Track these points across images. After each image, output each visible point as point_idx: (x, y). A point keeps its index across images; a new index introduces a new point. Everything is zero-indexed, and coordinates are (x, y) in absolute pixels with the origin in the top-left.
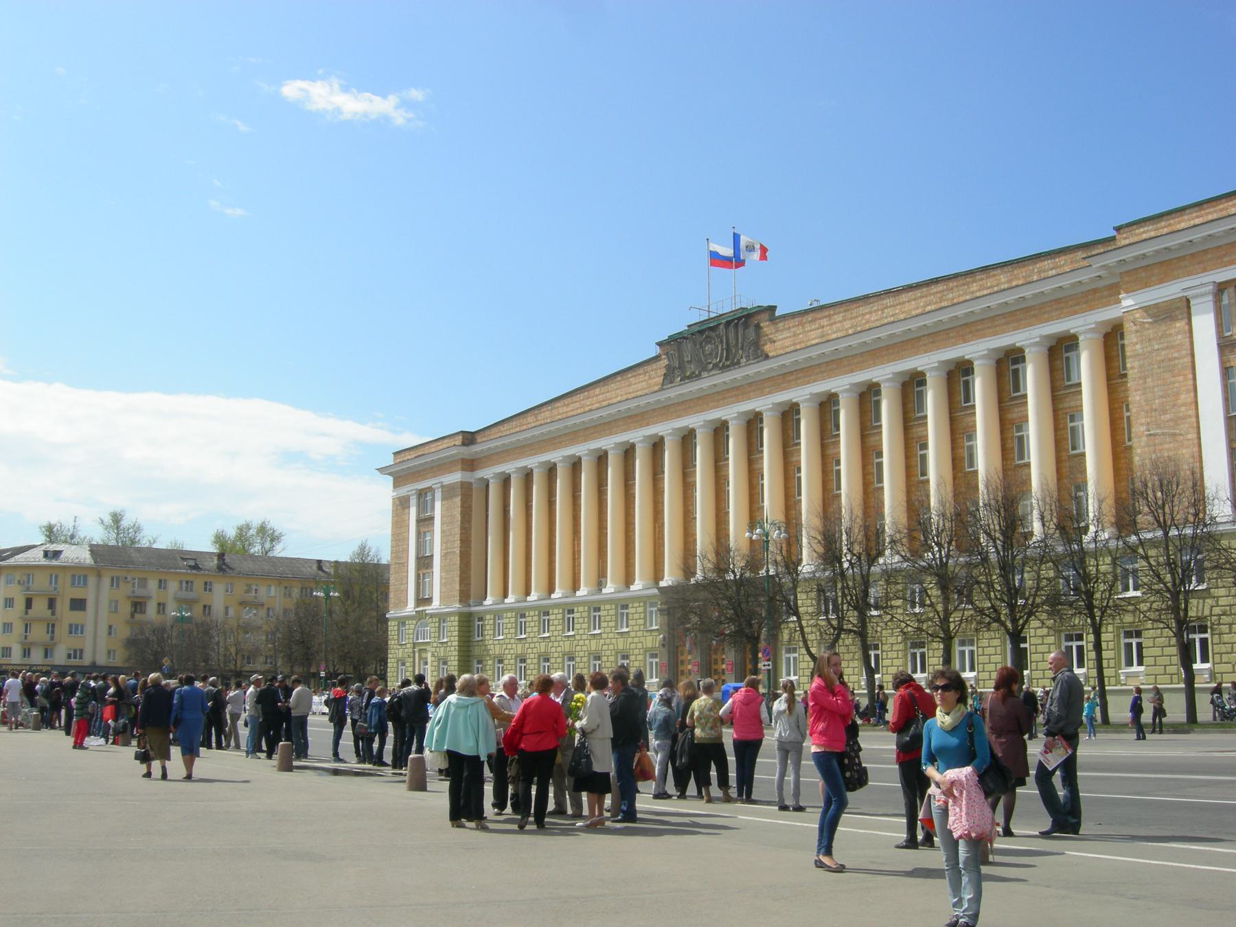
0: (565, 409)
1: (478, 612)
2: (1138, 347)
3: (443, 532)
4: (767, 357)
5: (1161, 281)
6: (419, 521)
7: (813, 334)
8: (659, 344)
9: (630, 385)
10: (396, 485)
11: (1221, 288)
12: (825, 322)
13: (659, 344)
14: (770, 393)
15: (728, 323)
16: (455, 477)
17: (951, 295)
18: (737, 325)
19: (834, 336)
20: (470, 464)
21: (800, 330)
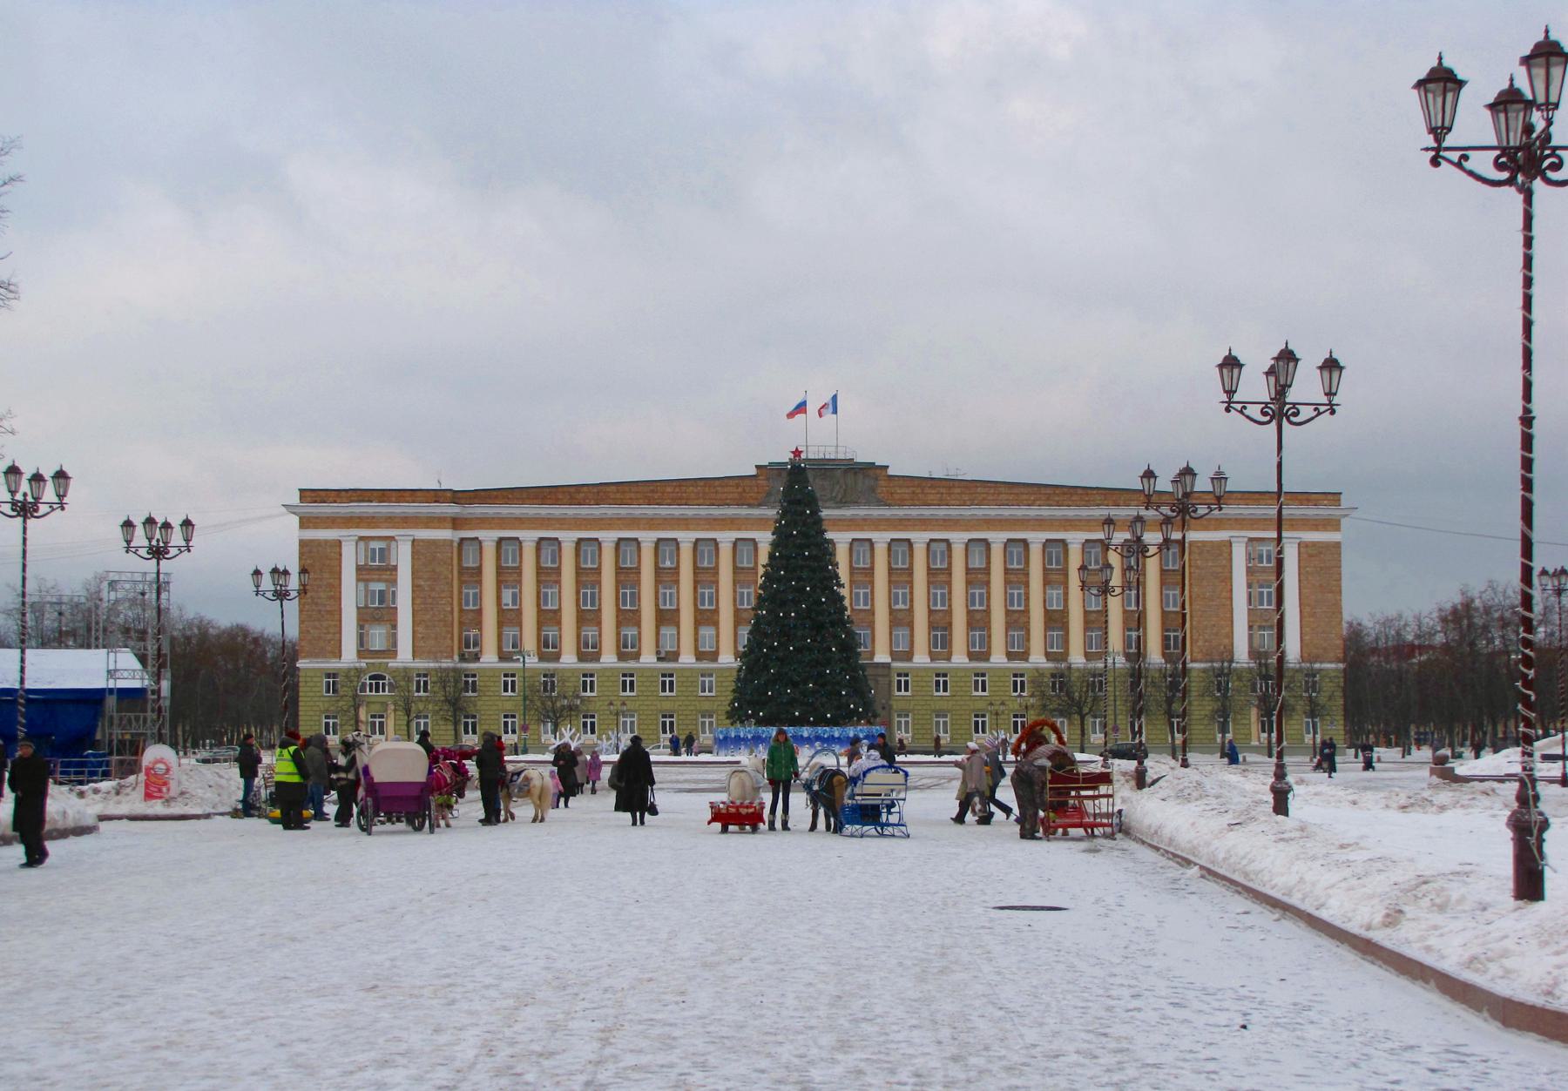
0: (618, 496)
1: (466, 670)
2: (1199, 562)
3: (416, 588)
4: (881, 503)
5: (1216, 529)
6: (359, 569)
7: (932, 497)
8: (757, 466)
9: (716, 492)
10: (305, 522)
11: (1251, 540)
12: (944, 491)
13: (757, 466)
14: (885, 530)
15: (846, 471)
16: (445, 534)
17: (1057, 498)
18: (855, 473)
19: (953, 502)
20: (456, 523)
21: (919, 490)
